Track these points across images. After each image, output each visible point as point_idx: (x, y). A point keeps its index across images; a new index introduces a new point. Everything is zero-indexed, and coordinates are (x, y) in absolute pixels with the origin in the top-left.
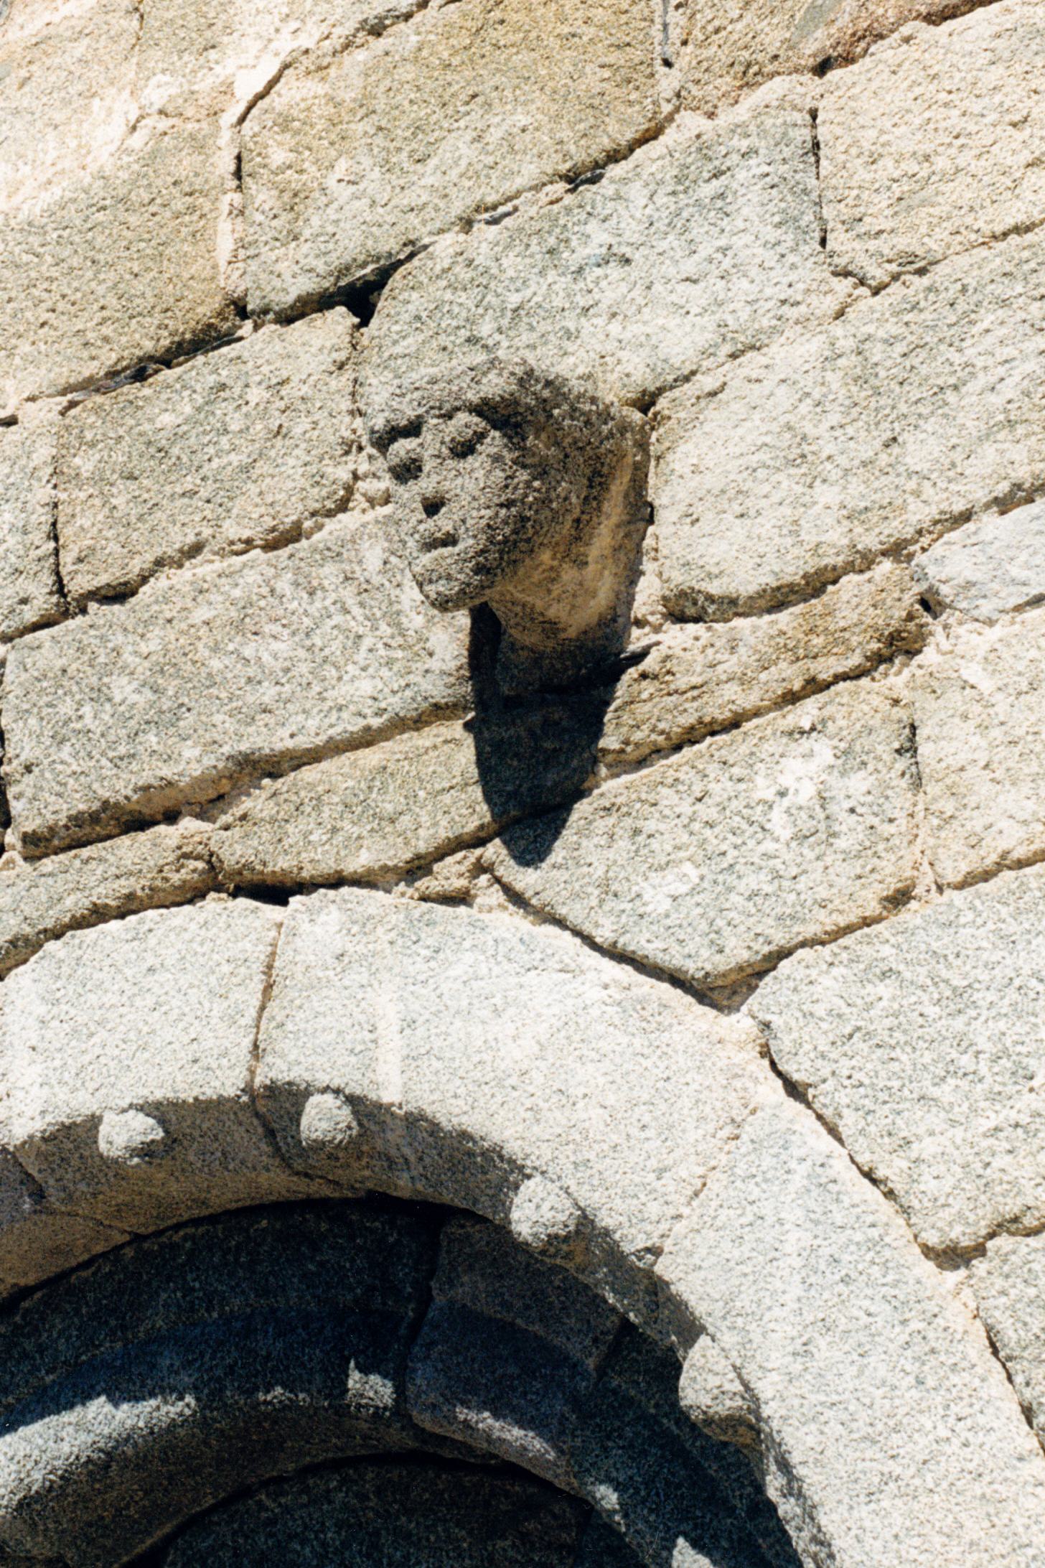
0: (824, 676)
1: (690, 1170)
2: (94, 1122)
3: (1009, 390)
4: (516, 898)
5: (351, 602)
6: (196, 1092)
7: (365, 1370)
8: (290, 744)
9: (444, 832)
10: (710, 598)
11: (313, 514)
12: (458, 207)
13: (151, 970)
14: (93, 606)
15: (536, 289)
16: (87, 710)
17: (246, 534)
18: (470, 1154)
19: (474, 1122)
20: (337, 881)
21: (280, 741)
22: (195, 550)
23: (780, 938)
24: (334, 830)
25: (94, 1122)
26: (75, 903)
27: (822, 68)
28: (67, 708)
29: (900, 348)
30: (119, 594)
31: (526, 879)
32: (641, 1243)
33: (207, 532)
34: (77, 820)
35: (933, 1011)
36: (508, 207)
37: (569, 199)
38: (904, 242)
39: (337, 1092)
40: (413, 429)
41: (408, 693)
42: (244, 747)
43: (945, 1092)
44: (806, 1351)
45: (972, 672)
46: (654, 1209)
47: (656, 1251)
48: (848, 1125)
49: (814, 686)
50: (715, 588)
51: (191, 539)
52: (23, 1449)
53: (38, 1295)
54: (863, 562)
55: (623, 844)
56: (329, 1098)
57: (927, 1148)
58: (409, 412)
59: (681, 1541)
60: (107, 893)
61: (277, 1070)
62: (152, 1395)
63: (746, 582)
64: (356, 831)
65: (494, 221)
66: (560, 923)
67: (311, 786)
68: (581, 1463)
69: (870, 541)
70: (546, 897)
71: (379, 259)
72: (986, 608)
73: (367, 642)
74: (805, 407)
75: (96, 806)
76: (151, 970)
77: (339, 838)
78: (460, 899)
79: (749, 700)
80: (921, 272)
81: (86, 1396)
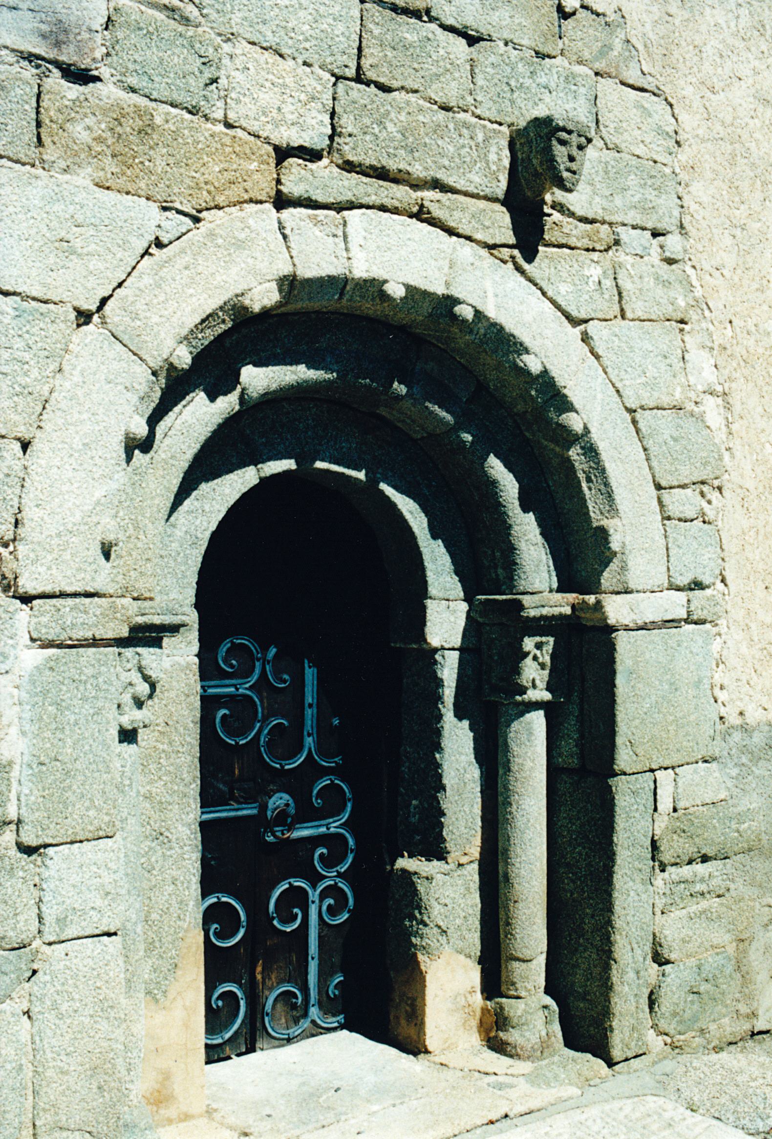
0: (597, 248)
1: (573, 368)
2: (386, 281)
3: (636, 199)
4: (518, 268)
5: (474, 148)
6: (426, 288)
7: (400, 383)
8: (454, 185)
9: (503, 241)
10: (568, 210)
11: (459, 107)
12: (506, 35)
13: (409, 239)
14: (372, 86)
15: (528, 82)
16: (375, 126)
17: (437, 99)
18: (510, 341)
19: (516, 333)
20: (469, 238)
21: (451, 181)
22: (416, 91)
23: (593, 316)
24: (470, 222)
25: (386, 281)
26: (372, 199)
27: (597, 74)
28: (367, 121)
29: (614, 170)
30: (385, 89)
31: (526, 266)
32: (563, 384)
33: (421, 89)
34: (372, 167)
35: (627, 350)
36: (519, 48)
37: (535, 59)
38: (617, 142)
39: (473, 307)
40: (570, 132)
41: (492, 190)
42: (438, 176)
43: (629, 369)
44: (602, 424)
45: (629, 267)
46: (566, 376)
47: (565, 387)
48: (609, 370)
49: (594, 250)
50: (572, 208)
51: (416, 87)
52: (272, 375)
53: (275, 319)
54: (603, 222)
55: (553, 269)
56: (470, 307)
57: (627, 383)
58: (570, 127)
59: (492, 455)
60: (388, 202)
61: (456, 292)
62: (323, 369)
63: (580, 212)
64: (476, 226)
65: (515, 49)
66: (536, 285)
67: (461, 203)
68: (459, 426)
69: (607, 218)
70: (533, 275)
71: (478, 32)
72: (627, 251)
73: (478, 165)
74: (593, 171)
75: (379, 166)
76: (409, 239)
77: (471, 225)
78: (504, 262)
79: (579, 245)
80: (618, 152)
81: (297, 363)
